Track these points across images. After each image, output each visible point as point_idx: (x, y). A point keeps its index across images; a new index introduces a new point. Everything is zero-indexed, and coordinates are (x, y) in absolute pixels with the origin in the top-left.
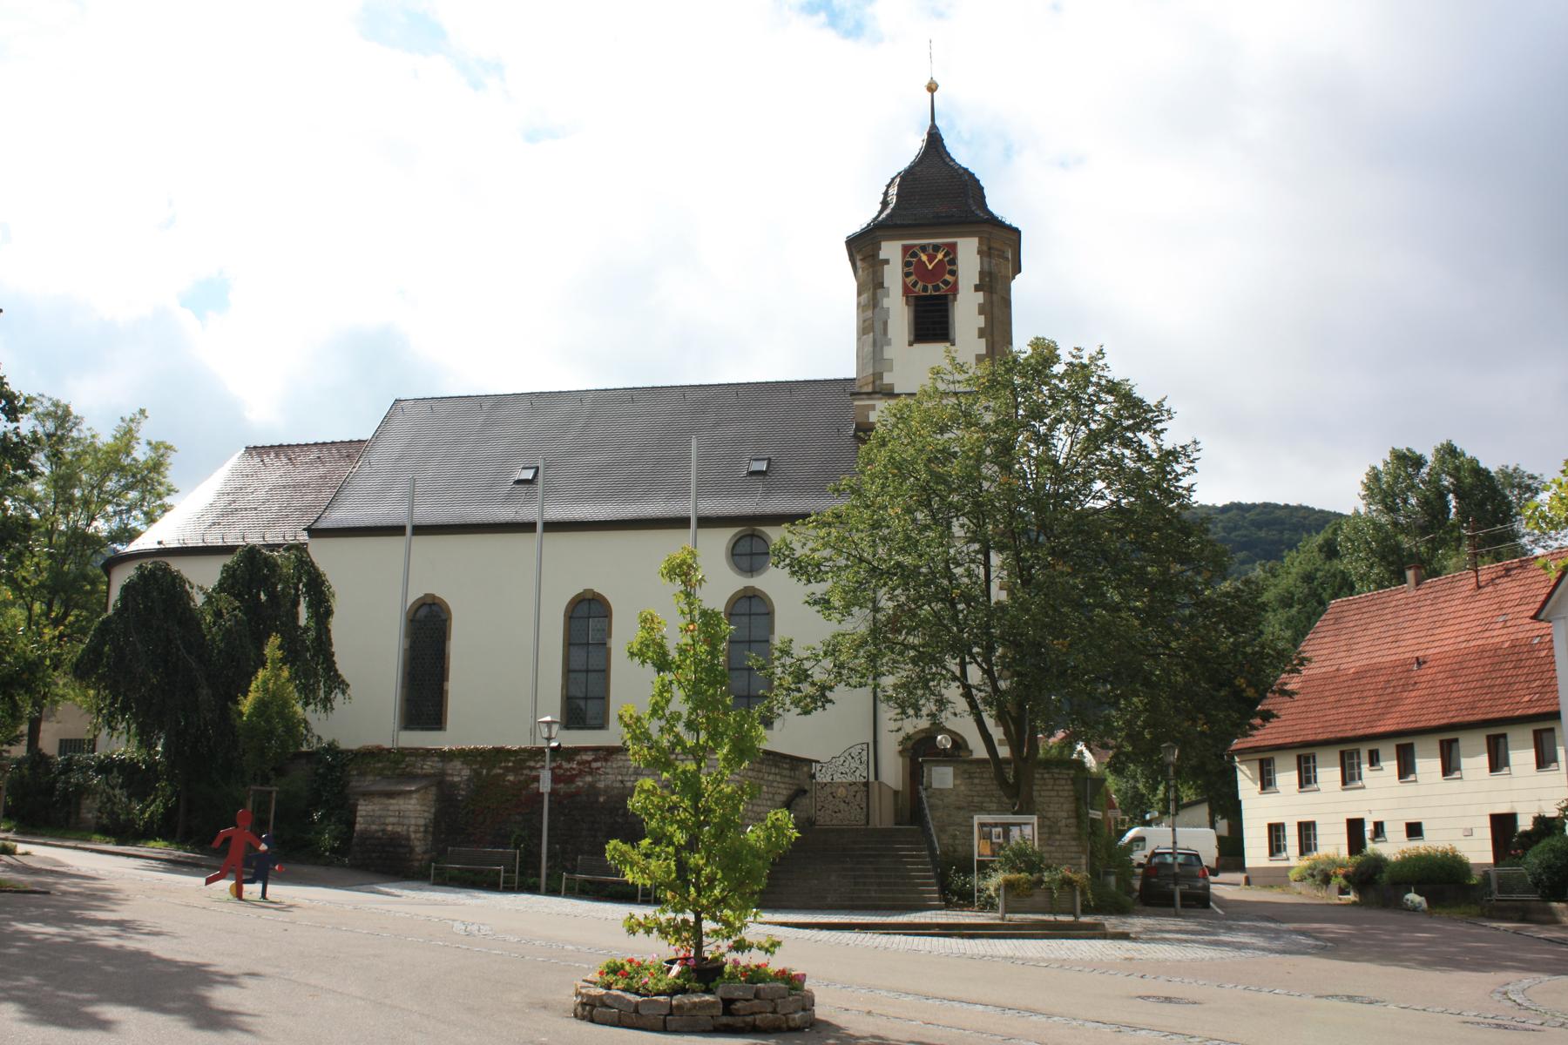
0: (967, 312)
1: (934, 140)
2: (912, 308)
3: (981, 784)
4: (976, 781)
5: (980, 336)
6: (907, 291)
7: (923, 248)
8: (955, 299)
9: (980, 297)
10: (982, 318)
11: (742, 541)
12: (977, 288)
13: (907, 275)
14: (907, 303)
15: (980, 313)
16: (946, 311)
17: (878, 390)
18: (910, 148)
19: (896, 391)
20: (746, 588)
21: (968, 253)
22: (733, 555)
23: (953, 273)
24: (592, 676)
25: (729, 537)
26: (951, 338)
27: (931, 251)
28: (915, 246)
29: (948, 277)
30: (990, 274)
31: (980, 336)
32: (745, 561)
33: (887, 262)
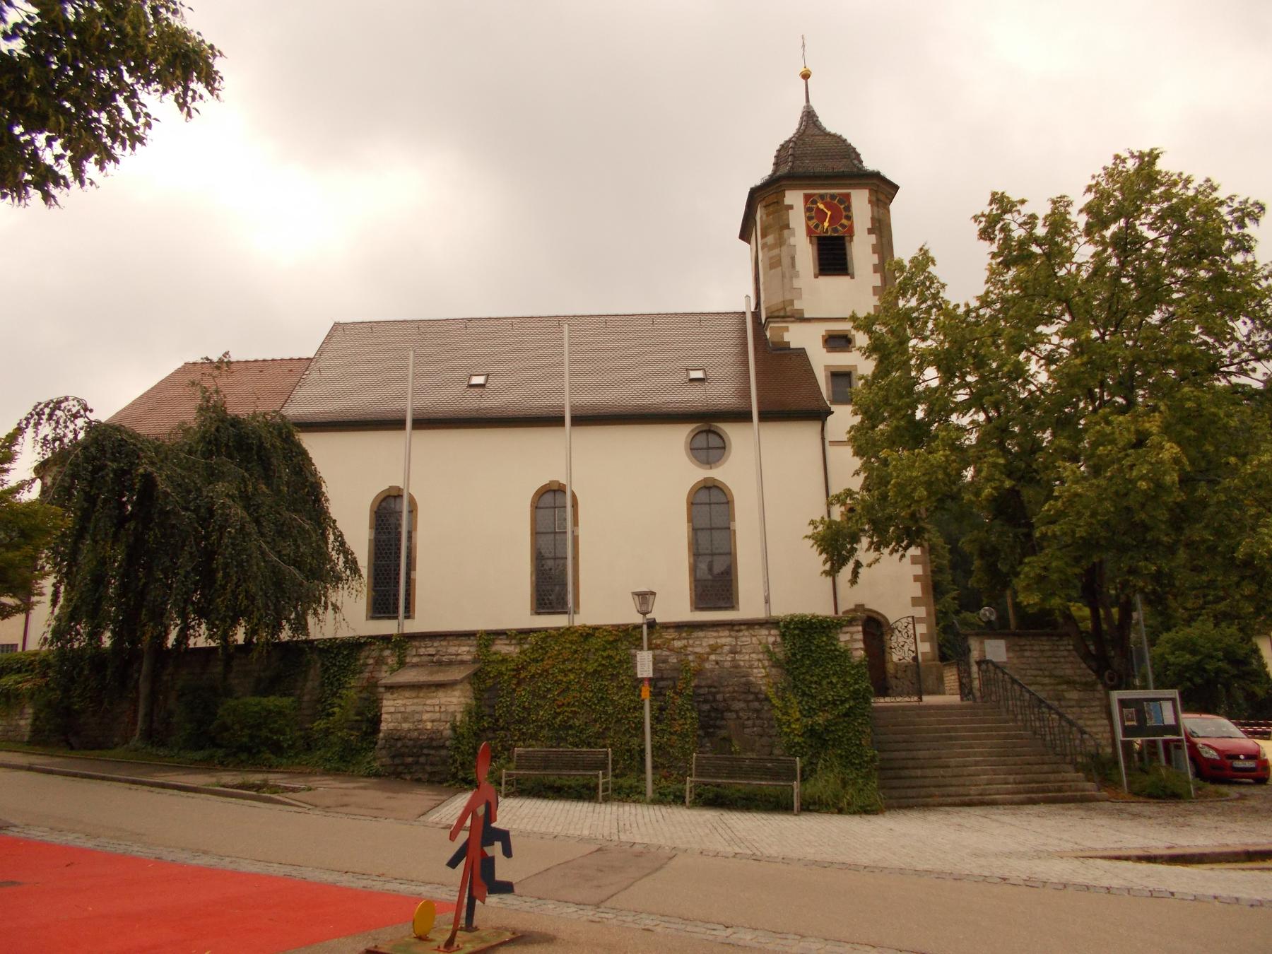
0: (861, 250)
1: (809, 117)
2: (815, 247)
3: (1031, 657)
4: (1027, 654)
5: (875, 272)
6: (810, 232)
7: (822, 197)
8: (851, 240)
9: (873, 239)
10: (876, 256)
11: (698, 437)
12: (870, 231)
13: (809, 218)
14: (811, 242)
15: (874, 252)
16: (845, 254)
17: (789, 314)
18: (789, 128)
19: (806, 316)
20: (706, 480)
21: (860, 202)
22: (691, 449)
23: (849, 218)
24: (716, 534)
25: (687, 433)
26: (850, 271)
27: (828, 200)
28: (815, 195)
29: (844, 221)
30: (879, 221)
31: (875, 272)
32: (703, 454)
33: (791, 207)
